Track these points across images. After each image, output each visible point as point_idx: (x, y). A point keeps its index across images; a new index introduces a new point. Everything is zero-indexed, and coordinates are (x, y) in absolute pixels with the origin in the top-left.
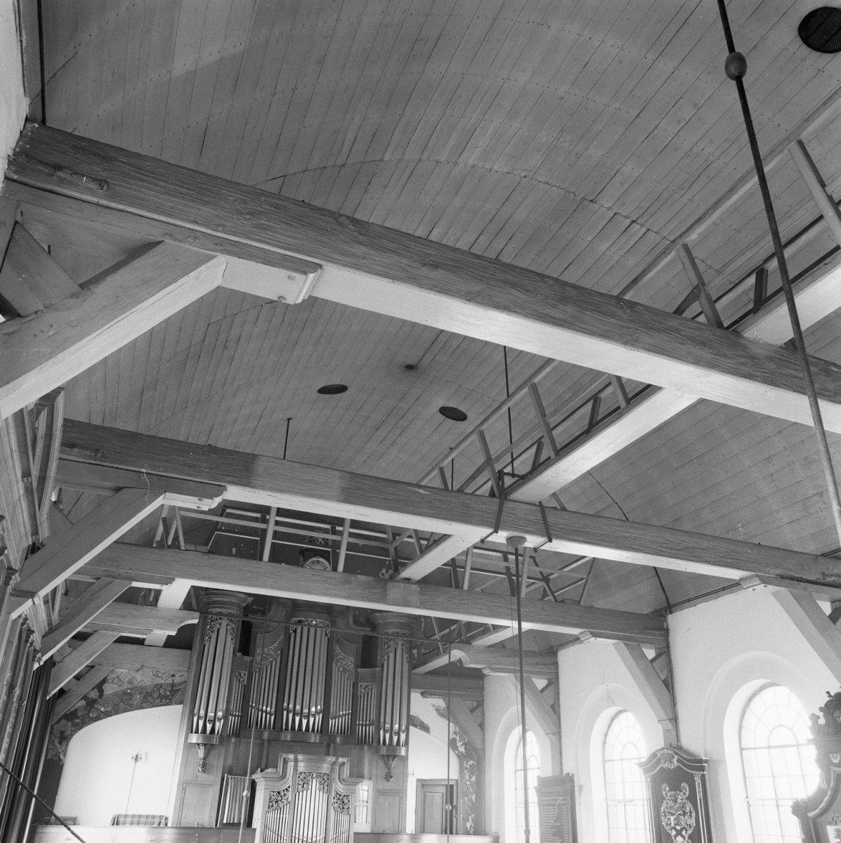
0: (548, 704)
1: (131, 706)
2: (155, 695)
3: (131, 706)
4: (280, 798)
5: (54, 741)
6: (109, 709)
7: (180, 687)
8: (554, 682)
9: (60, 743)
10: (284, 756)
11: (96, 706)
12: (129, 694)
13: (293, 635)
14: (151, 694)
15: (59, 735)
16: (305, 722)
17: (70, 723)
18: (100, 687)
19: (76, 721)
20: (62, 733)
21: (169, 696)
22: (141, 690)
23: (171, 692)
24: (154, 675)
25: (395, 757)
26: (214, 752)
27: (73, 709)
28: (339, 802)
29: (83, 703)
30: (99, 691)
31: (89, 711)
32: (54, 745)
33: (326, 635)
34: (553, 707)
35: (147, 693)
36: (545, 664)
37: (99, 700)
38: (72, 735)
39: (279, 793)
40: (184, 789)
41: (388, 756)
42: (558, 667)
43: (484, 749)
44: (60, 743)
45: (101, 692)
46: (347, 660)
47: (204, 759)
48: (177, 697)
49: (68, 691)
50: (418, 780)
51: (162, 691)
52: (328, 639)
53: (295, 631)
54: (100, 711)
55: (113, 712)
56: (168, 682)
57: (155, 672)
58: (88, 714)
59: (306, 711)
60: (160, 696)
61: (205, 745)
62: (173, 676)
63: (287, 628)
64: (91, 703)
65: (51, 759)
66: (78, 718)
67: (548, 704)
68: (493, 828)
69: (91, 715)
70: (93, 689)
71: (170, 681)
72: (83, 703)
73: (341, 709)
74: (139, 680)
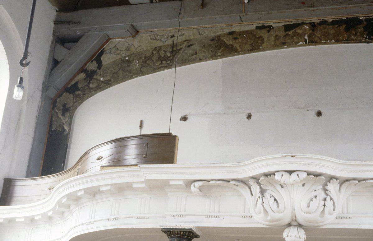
1: (130, 72)
2: (155, 58)
3: (130, 72)
5: (57, 114)
6: (108, 78)
7: (181, 47)
9: (63, 115)
11: (95, 77)
12: (128, 61)
14: (150, 58)
15: (62, 108)
17: (72, 96)
18: (98, 57)
19: (77, 93)
20: (65, 105)
21: (169, 57)
22: (139, 55)
23: (172, 52)
24: (152, 39)
27: (73, 82)
29: (82, 75)
30: (97, 63)
31: (89, 83)
32: (58, 117)
35: (145, 57)
37: (98, 71)
38: (75, 107)
44: (63, 115)
45: (99, 63)
48: (179, 56)
49: (61, 61)
51: (162, 54)
54: (100, 81)
55: (112, 80)
56: (167, 43)
57: (152, 37)
58: (88, 86)
60: (161, 59)
62: (173, 36)
64: (90, 75)
65: (55, 131)
66: (79, 90)
69: (91, 86)
70: (90, 60)
71: (170, 42)
72: (82, 75)
74: (136, 47)
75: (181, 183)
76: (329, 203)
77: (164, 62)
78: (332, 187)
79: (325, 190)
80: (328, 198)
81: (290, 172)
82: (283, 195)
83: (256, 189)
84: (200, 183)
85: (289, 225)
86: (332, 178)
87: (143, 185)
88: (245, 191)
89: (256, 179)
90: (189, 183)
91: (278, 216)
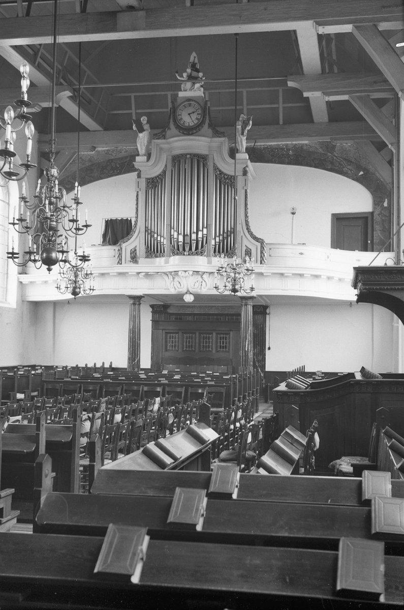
50: (334, 215)
51: (113, 164)
75: (135, 273)
77: (115, 171)
78: (205, 276)
81: (185, 271)
83: (171, 277)
84: (144, 274)
85: (186, 293)
86: (204, 273)
87: (115, 274)
88: (166, 277)
89: (171, 272)
90: (138, 273)
91: (180, 290)
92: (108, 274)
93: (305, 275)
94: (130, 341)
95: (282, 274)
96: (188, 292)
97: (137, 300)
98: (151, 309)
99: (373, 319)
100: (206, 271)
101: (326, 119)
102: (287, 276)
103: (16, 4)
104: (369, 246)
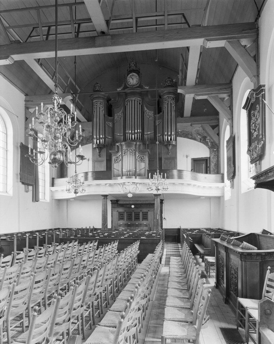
0: (226, 106)
3: (83, 143)
4: (117, 159)
8: (231, 96)
10: (117, 144)
13: (127, 106)
16: (133, 136)
25: (170, 145)
26: (103, 150)
28: (140, 158)
33: (140, 104)
34: (230, 107)
36: (226, 89)
39: (117, 157)
40: (94, 163)
41: (167, 145)
42: (232, 89)
43: (219, 143)
46: (149, 113)
47: (99, 153)
52: (141, 106)
53: (127, 104)
59: (133, 132)
61: (98, 148)
63: (124, 104)
67: (226, 106)
68: (222, 172)
73: (148, 131)
75: (104, 184)
76: (137, 188)
78: (137, 185)
79: (136, 186)
80: (137, 188)
81: (129, 183)
82: (127, 187)
83: (121, 186)
84: (109, 184)
87: (95, 185)
88: (119, 186)
90: (106, 184)
91: (126, 191)
92: (92, 185)
93: (184, 184)
94: (102, 216)
95: (174, 184)
96: (130, 193)
97: (105, 196)
98: (111, 202)
99: (210, 204)
100: (138, 182)
101: (189, 115)
102: (176, 185)
103: (40, 37)
104: (208, 172)
